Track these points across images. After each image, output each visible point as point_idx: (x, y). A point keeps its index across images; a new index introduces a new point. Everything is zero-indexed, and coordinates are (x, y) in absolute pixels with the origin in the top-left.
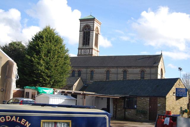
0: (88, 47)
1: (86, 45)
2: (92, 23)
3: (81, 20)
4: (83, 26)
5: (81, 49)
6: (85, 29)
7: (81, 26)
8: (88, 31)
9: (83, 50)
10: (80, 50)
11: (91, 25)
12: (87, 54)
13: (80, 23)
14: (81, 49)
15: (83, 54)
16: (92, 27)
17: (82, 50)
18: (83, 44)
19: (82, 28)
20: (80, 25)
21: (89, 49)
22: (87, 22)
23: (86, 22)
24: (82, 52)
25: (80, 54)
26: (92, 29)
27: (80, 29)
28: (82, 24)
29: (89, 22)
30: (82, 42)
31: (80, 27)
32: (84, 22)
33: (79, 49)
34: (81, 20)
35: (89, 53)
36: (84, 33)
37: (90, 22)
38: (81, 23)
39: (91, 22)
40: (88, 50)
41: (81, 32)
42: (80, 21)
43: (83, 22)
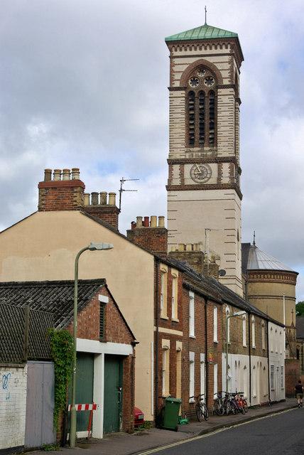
2: (227, 58)
3: (172, 44)
4: (184, 68)
5: (182, 162)
6: (194, 81)
7: (175, 69)
8: (208, 86)
9: (191, 166)
10: (176, 168)
11: (219, 67)
12: (213, 181)
13: (172, 57)
14: (182, 162)
15: (193, 183)
16: (225, 74)
17: (188, 167)
18: (191, 142)
19: (178, 76)
20: (172, 65)
21: (220, 161)
22: (198, 52)
23: (193, 52)
24: (187, 175)
25: (177, 182)
26: (226, 82)
27: (172, 80)
28: (176, 61)
29: (208, 52)
30: (181, 130)
31: (172, 71)
32: (188, 53)
33: (171, 162)
35: (219, 179)
36: (191, 94)
37: (214, 51)
39: (219, 51)
40: (214, 166)
42: (171, 50)
43: (183, 53)
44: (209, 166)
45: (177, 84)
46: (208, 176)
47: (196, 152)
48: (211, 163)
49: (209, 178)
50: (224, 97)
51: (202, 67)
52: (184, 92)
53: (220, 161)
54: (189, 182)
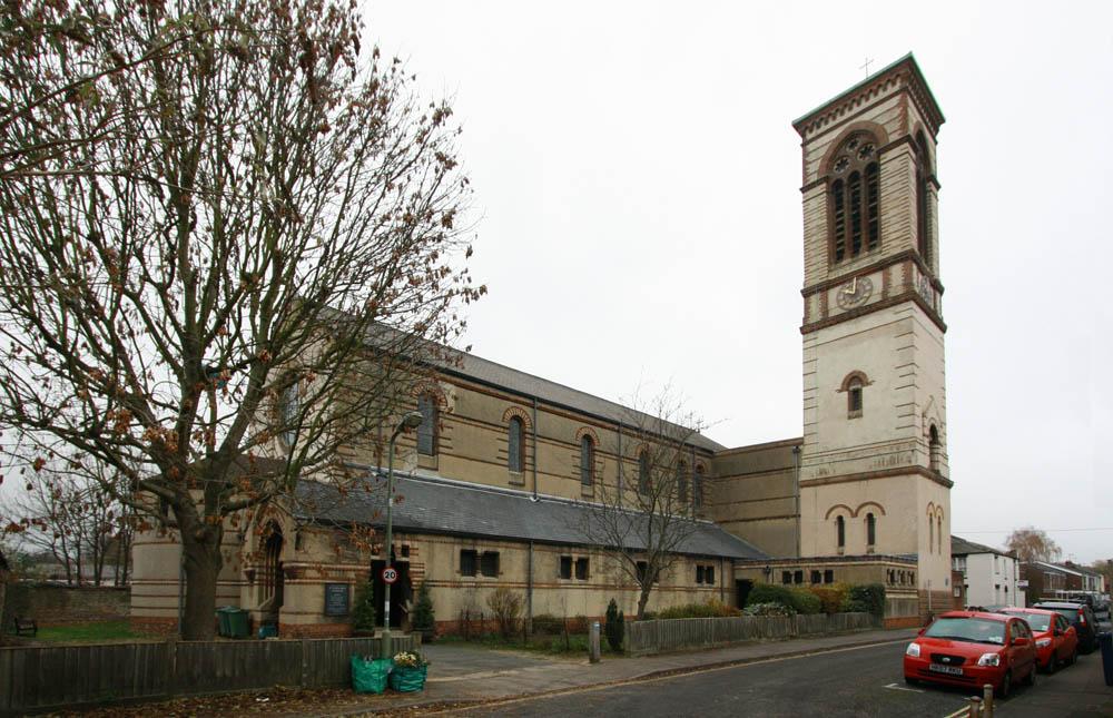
0: (878, 258)
1: (856, 251)
4: (822, 152)
8: (862, 163)
12: (876, 299)
15: (840, 311)
19: (814, 167)
20: (806, 154)
21: (883, 266)
28: (811, 147)
30: (821, 237)
31: (805, 163)
34: (802, 126)
36: (835, 189)
38: (809, 136)
40: (876, 279)
41: (811, 193)
42: (803, 136)
44: (870, 283)
45: (814, 178)
46: (867, 295)
47: (849, 268)
48: (869, 273)
49: (868, 298)
50: (896, 171)
51: (850, 138)
52: (824, 185)
53: (883, 266)
54: (834, 311)
